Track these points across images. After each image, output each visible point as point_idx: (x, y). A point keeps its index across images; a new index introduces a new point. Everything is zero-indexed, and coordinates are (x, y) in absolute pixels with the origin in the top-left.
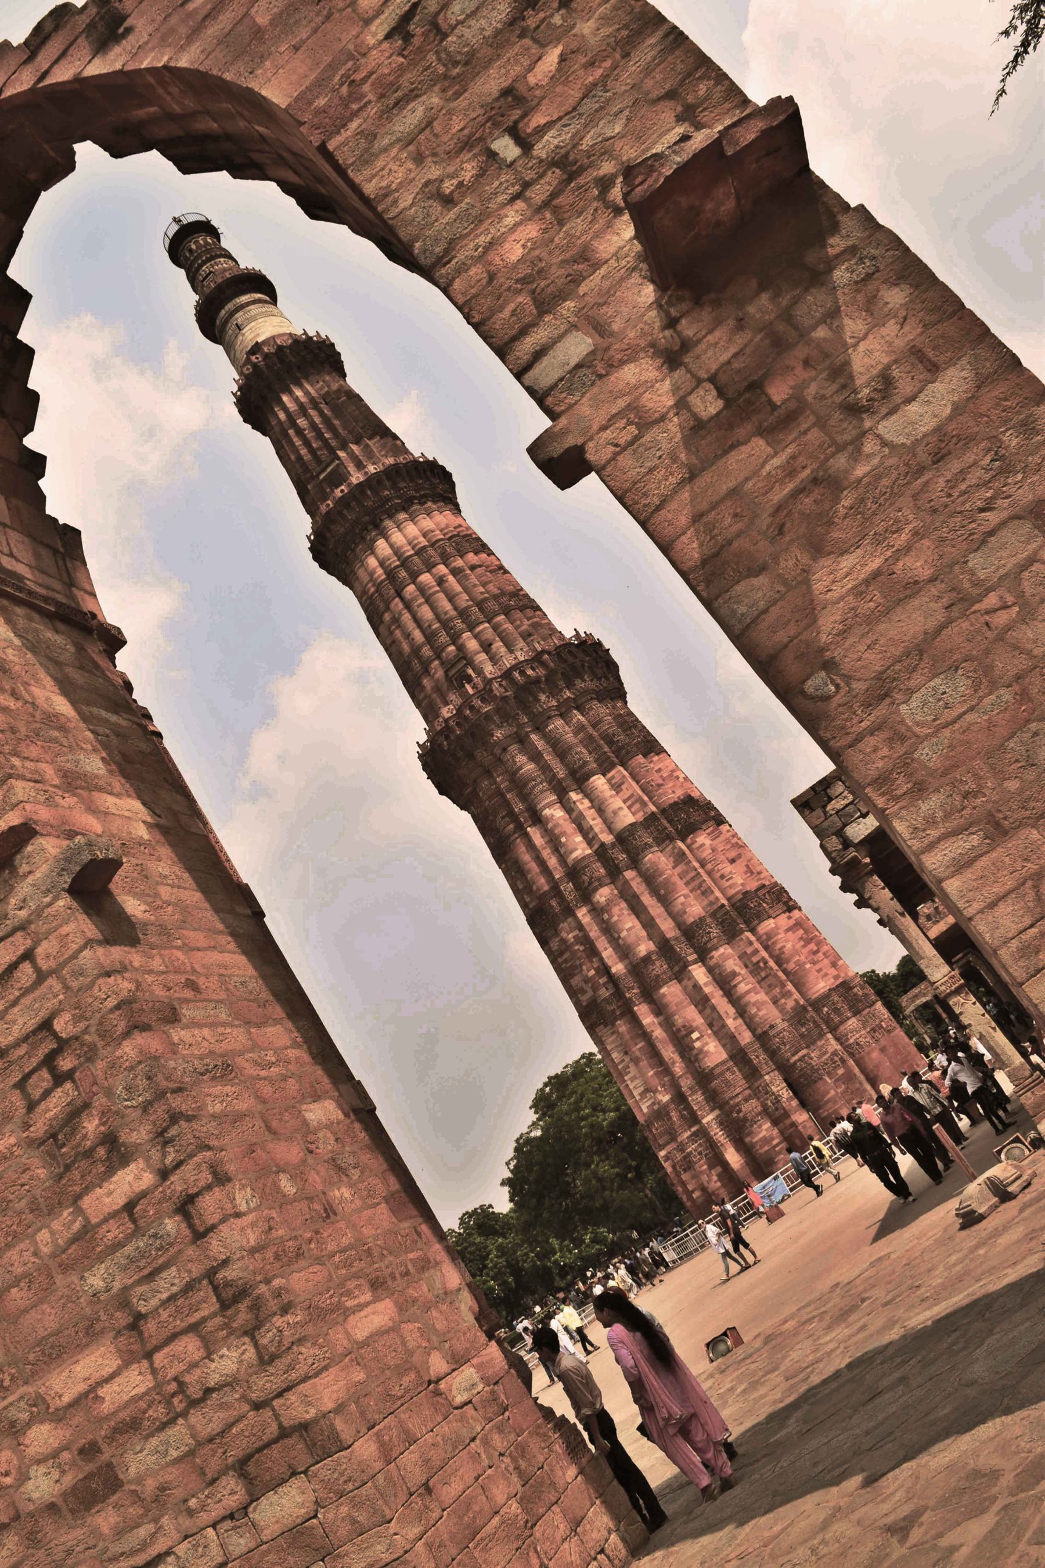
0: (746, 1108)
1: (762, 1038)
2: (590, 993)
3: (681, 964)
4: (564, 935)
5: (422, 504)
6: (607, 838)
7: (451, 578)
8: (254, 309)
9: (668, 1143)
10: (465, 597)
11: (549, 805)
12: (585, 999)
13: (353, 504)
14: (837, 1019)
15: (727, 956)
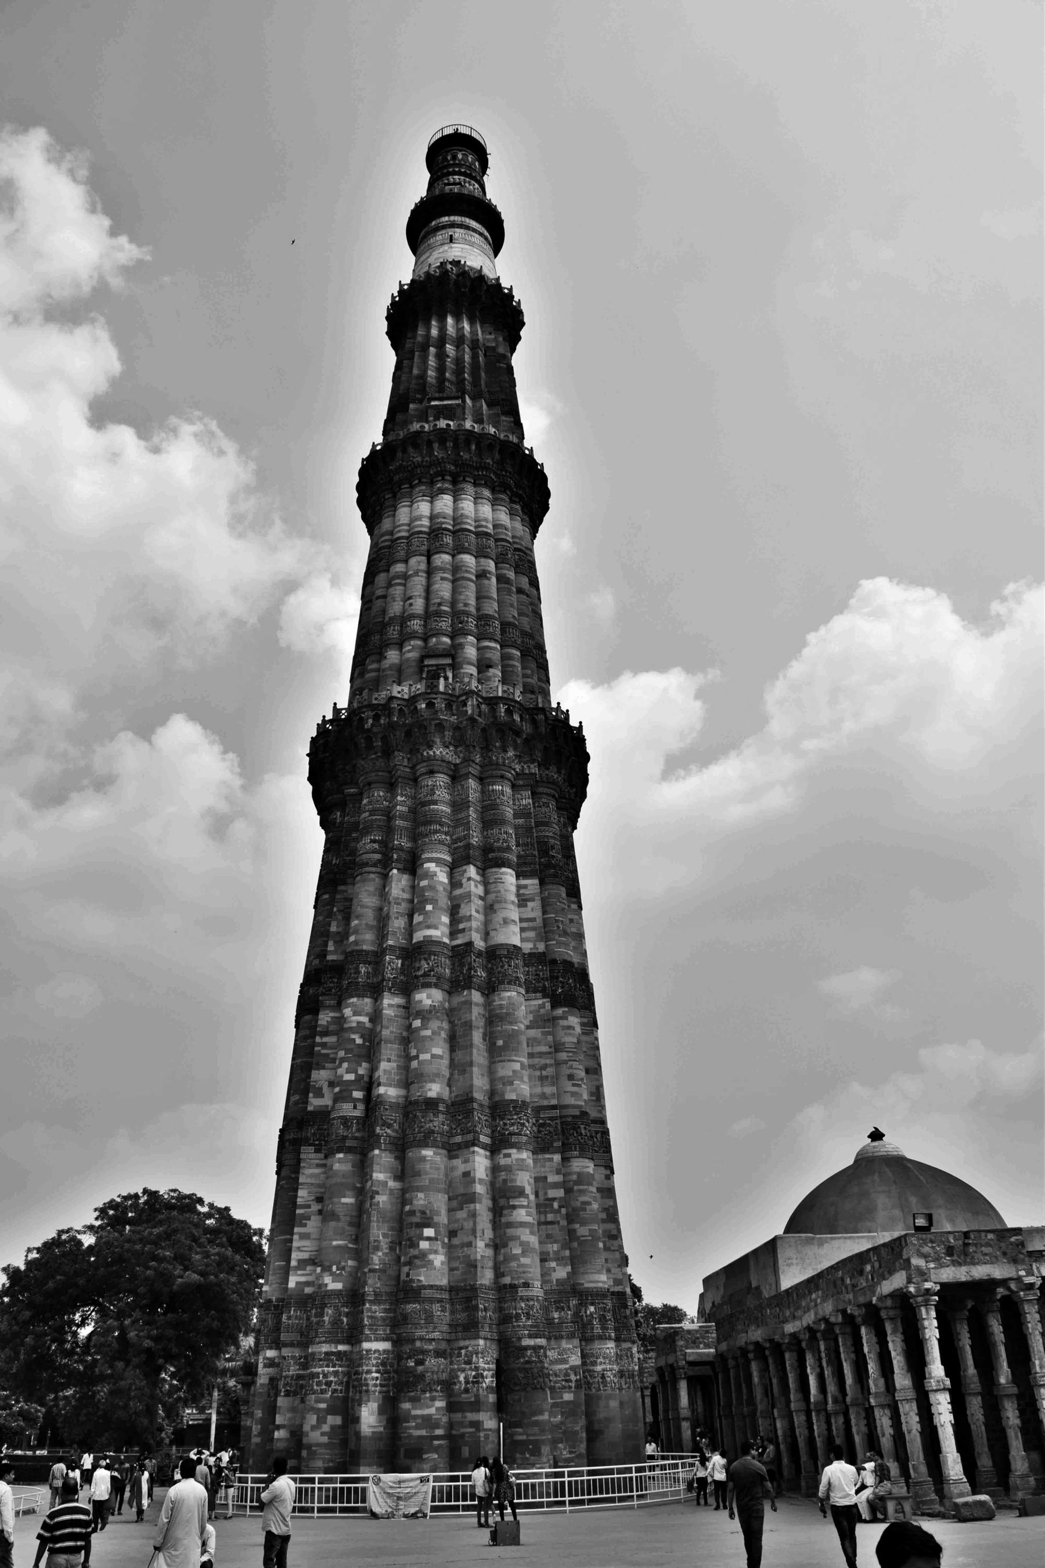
0: (431, 1362)
1: (506, 1292)
2: (326, 1101)
3: (470, 1137)
4: (348, 1012)
5: (512, 501)
6: (479, 944)
7: (494, 580)
8: (476, 238)
9: (292, 1345)
10: (495, 605)
11: (438, 861)
12: (315, 1103)
13: (450, 444)
14: (598, 1330)
15: (524, 1164)
